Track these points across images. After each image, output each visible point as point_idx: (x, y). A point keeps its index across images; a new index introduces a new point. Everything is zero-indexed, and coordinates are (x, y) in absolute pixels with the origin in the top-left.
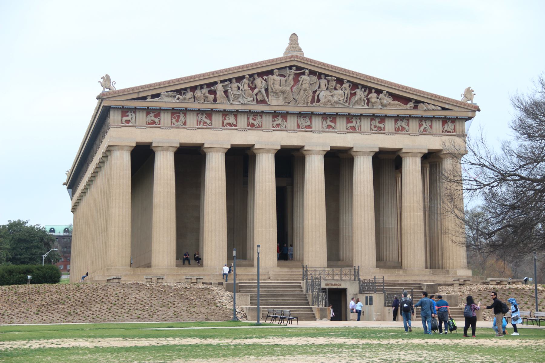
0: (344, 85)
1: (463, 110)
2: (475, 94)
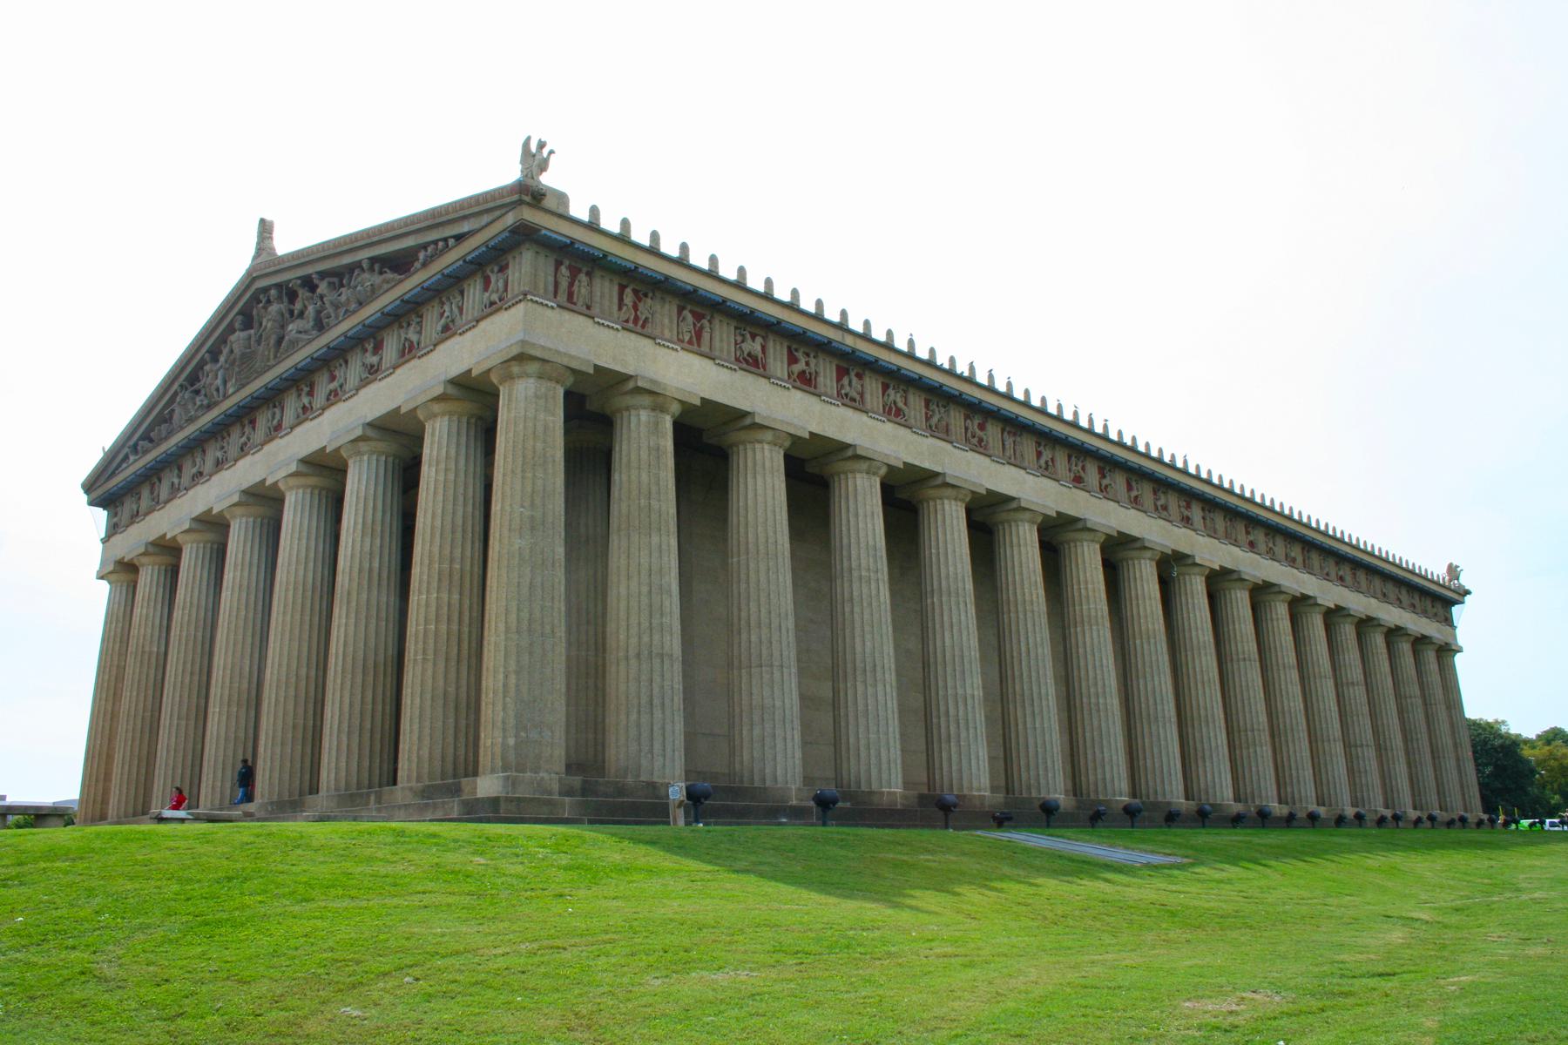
0: (319, 291)
1: (498, 213)
2: (551, 152)
